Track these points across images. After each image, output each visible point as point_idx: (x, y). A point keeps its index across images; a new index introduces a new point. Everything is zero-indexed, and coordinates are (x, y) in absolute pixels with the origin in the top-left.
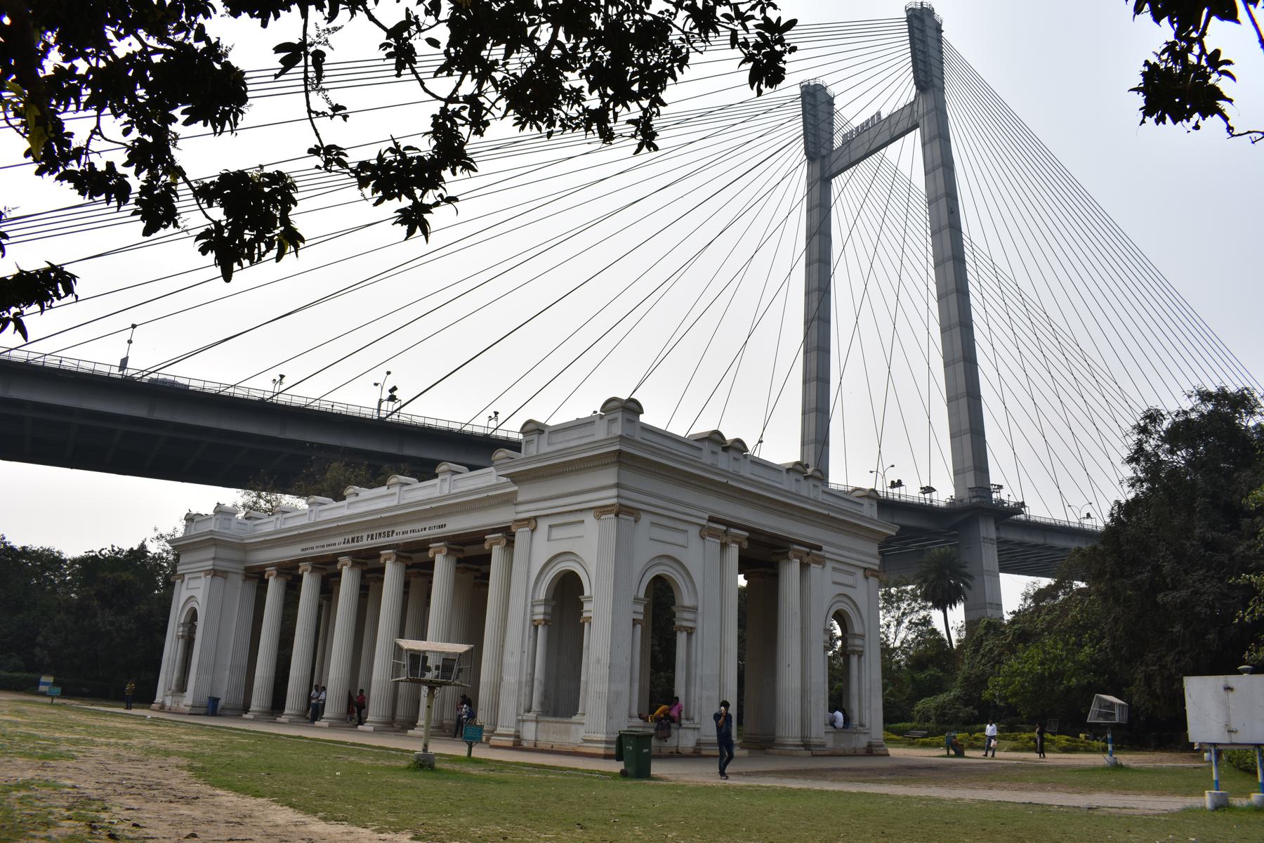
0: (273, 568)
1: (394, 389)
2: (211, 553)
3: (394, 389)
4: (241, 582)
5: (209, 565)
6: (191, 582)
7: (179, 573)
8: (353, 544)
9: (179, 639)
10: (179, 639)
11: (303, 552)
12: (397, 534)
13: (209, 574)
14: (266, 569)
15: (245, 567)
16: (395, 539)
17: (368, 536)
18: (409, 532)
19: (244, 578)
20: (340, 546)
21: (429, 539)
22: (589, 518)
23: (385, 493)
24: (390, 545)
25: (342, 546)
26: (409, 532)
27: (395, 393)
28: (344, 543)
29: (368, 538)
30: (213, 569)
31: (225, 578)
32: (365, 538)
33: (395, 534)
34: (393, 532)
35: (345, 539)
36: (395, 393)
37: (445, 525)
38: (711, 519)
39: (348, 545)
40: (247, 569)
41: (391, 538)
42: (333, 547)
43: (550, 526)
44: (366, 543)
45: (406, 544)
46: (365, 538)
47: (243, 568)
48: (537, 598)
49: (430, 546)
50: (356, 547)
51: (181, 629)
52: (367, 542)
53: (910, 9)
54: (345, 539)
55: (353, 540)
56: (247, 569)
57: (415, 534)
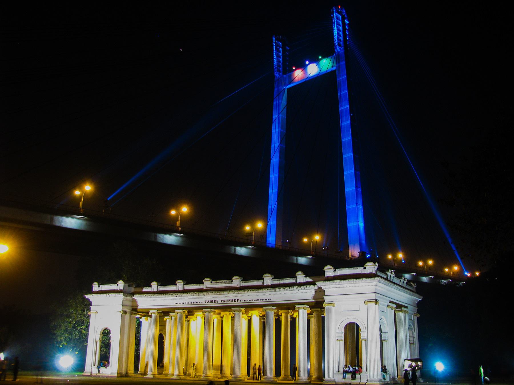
12: (241, 301)
17: (222, 301)
18: (248, 301)
26: (248, 301)
28: (205, 302)
32: (220, 302)
33: (239, 302)
34: (238, 300)
37: (270, 299)
38: (391, 302)
41: (236, 302)
46: (220, 302)
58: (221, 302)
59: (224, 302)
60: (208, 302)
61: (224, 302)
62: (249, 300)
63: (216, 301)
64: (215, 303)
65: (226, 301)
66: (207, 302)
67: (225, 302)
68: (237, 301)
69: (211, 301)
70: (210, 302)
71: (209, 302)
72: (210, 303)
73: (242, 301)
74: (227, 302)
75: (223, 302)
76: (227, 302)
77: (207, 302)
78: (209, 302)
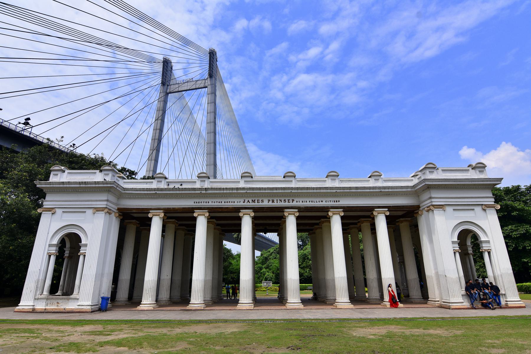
0: (162, 211)
1: (29, 119)
2: (104, 197)
3: (29, 119)
4: (114, 218)
5: (103, 204)
6: (65, 214)
7: (44, 207)
8: (253, 204)
9: (50, 256)
10: (50, 256)
11: (196, 204)
12: (297, 202)
13: (103, 211)
14: (150, 211)
15: (118, 208)
16: (295, 204)
17: (269, 201)
19: (117, 215)
20: (239, 204)
21: (345, 206)
22: (478, 209)
23: (282, 180)
24: (291, 207)
25: (242, 203)
26: (308, 202)
27: (29, 121)
28: (244, 202)
29: (268, 201)
30: (106, 208)
31: (110, 214)
34: (293, 201)
35: (245, 200)
36: (29, 121)
37: (339, 201)
39: (248, 203)
40: (119, 209)
42: (231, 204)
43: (454, 210)
44: (266, 203)
45: (305, 207)
47: (117, 209)
48: (453, 240)
49: (331, 210)
50: (256, 205)
51: (54, 248)
52: (268, 204)
53: (211, 50)
54: (245, 200)
55: (253, 201)
56: (118, 208)
57: (313, 203)
58: (268, 202)
59: (272, 203)
60: (248, 201)
61: (272, 203)
62: (310, 201)
63: (260, 201)
64: (258, 204)
65: (275, 201)
66: (246, 201)
67: (274, 202)
68: (292, 202)
69: (252, 200)
70: (251, 201)
71: (249, 203)
72: (251, 204)
73: (299, 201)
74: (277, 202)
75: (270, 203)
76: (277, 202)
77: (246, 201)
78: (249, 203)
